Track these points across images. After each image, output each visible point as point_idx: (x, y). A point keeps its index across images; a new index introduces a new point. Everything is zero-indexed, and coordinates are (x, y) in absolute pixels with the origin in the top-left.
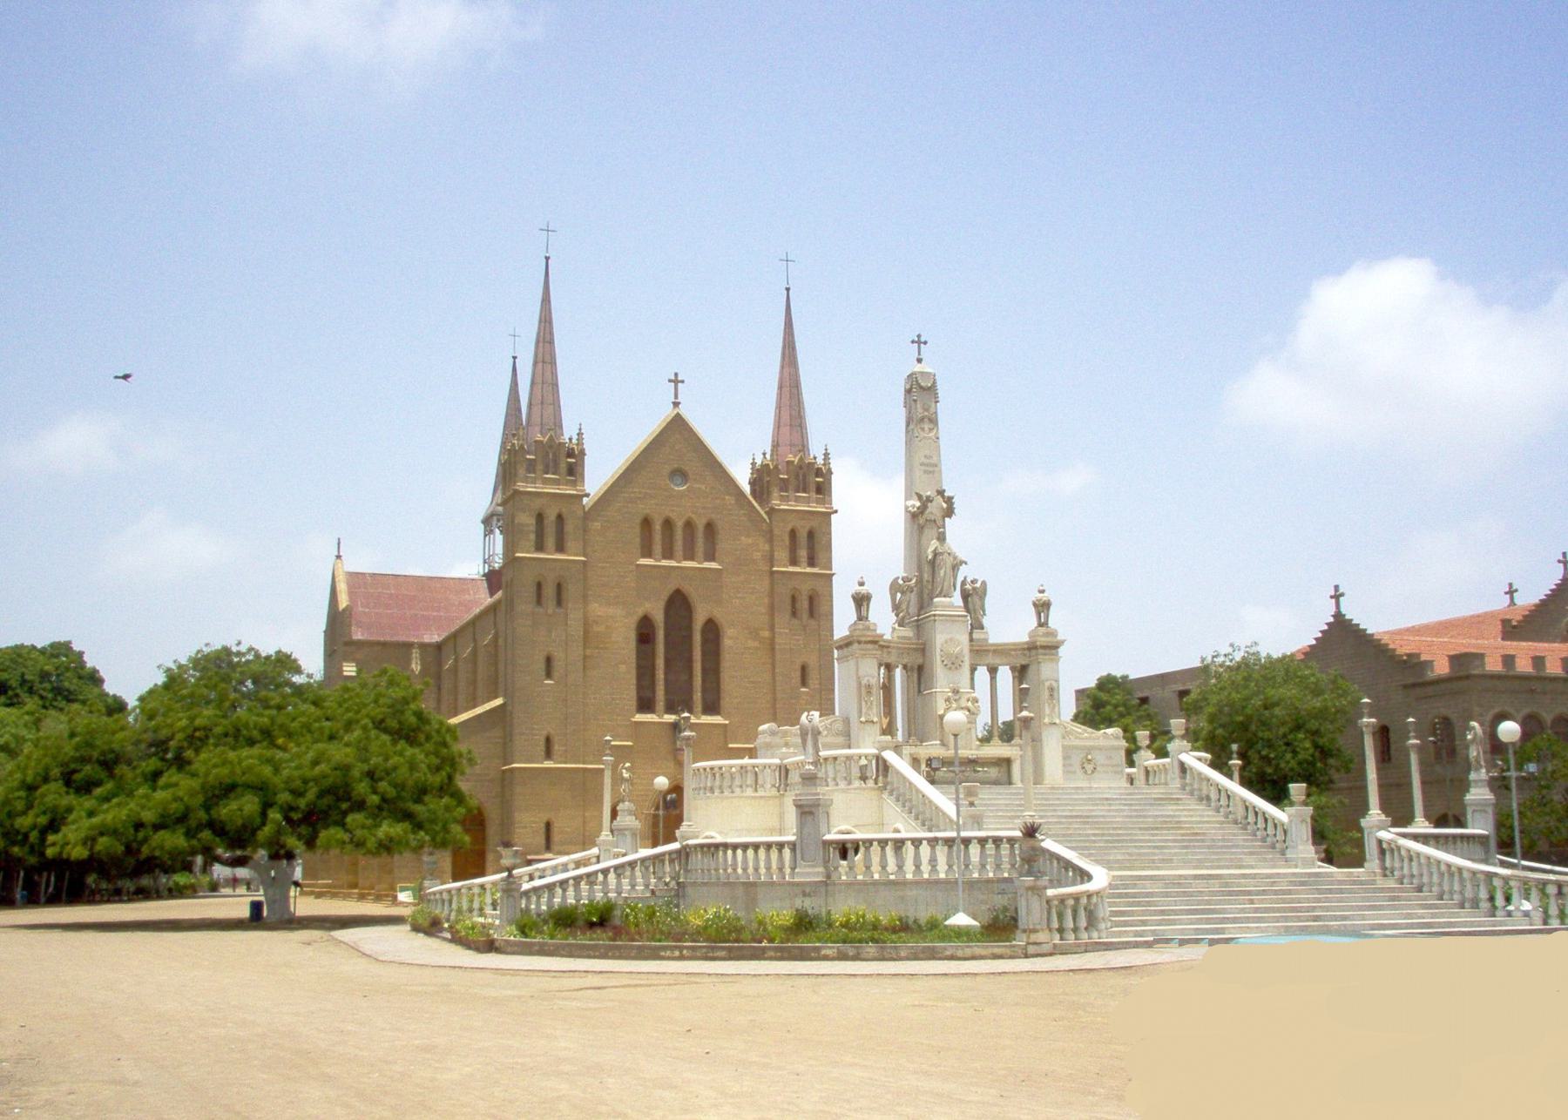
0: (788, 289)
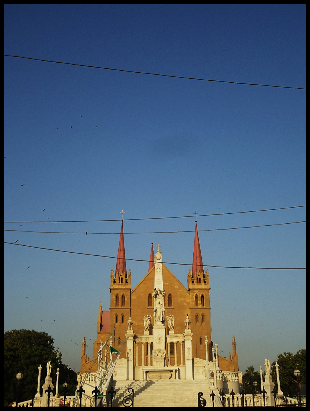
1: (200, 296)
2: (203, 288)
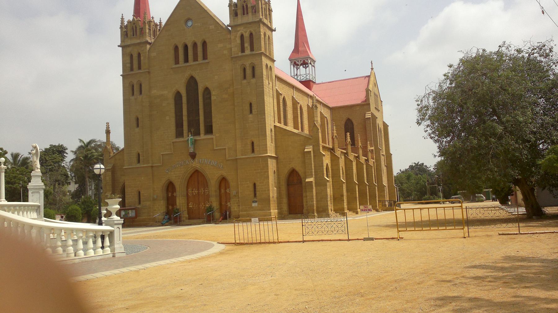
1: (247, 35)
2: (250, 20)
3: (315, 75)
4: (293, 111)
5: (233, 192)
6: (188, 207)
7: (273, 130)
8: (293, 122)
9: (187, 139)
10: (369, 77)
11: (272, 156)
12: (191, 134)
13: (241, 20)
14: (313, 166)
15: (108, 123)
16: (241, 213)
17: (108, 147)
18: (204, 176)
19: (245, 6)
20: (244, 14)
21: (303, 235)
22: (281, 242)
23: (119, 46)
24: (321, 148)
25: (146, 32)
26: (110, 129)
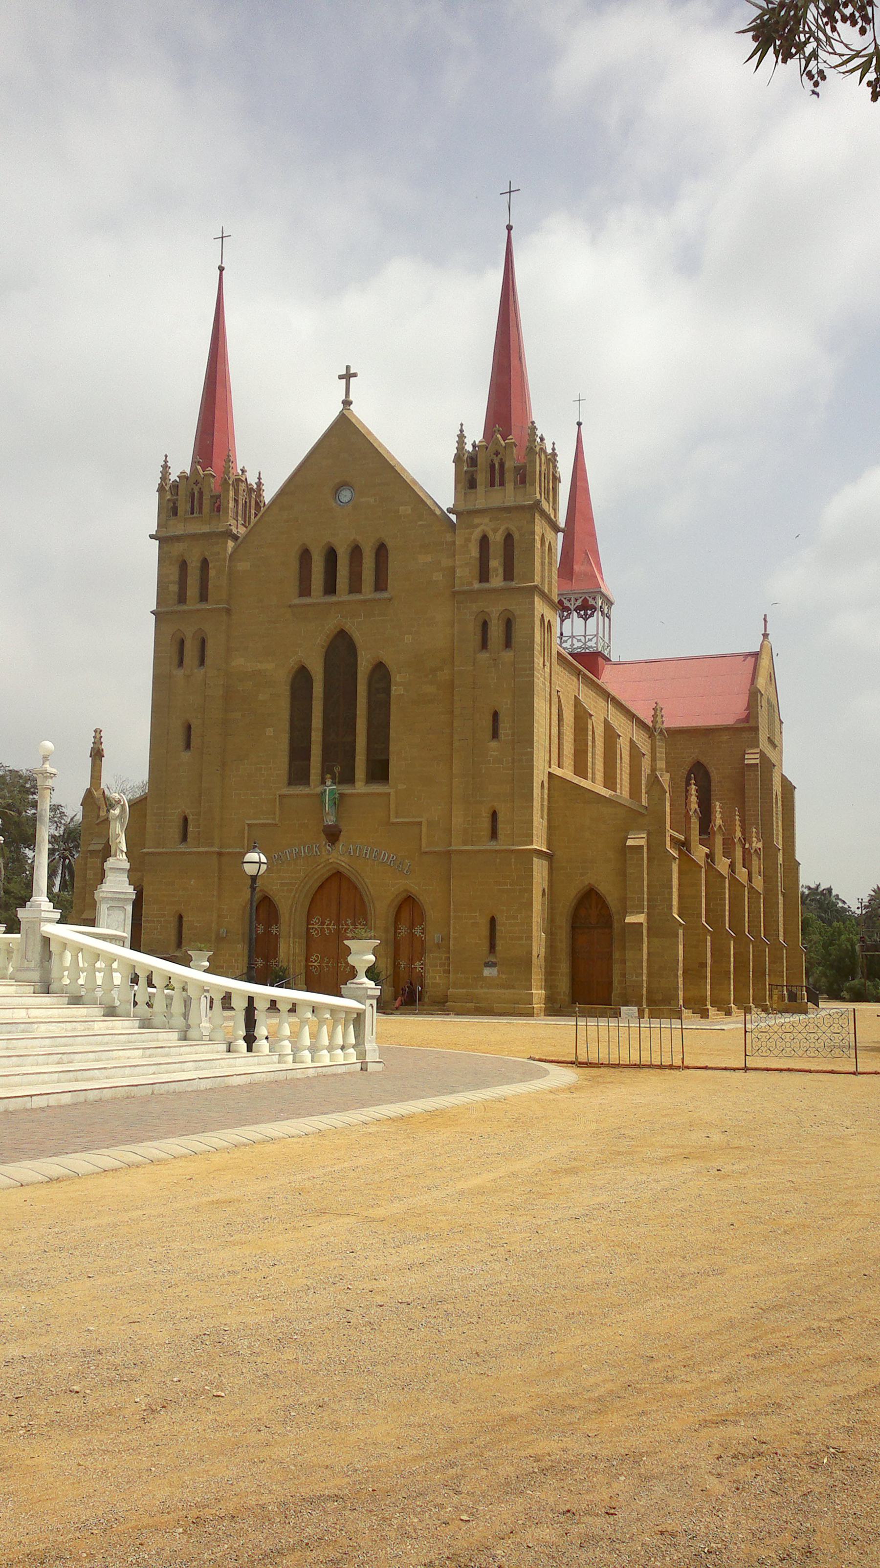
0: (509, 228)
1: (496, 538)
2: (510, 502)
3: (610, 639)
4: (575, 735)
5: (434, 935)
6: (307, 966)
7: (546, 785)
8: (573, 763)
9: (319, 789)
10: (756, 655)
11: (542, 851)
12: (332, 779)
13: (483, 498)
14: (645, 883)
15: (98, 732)
16: (451, 990)
17: (95, 793)
18: (356, 888)
19: (497, 466)
20: (492, 484)
21: (746, 1055)
22: (688, 1068)
23: (151, 537)
24: (668, 839)
25: (228, 507)
26: (103, 746)
